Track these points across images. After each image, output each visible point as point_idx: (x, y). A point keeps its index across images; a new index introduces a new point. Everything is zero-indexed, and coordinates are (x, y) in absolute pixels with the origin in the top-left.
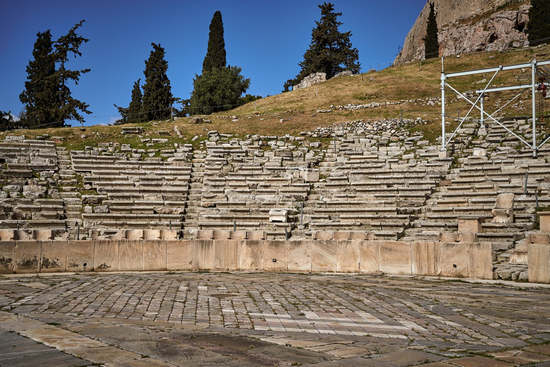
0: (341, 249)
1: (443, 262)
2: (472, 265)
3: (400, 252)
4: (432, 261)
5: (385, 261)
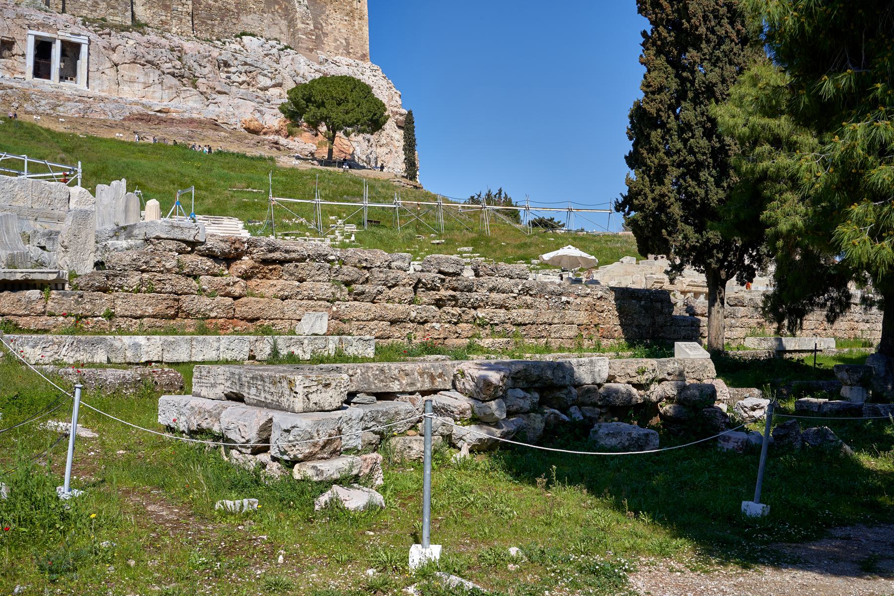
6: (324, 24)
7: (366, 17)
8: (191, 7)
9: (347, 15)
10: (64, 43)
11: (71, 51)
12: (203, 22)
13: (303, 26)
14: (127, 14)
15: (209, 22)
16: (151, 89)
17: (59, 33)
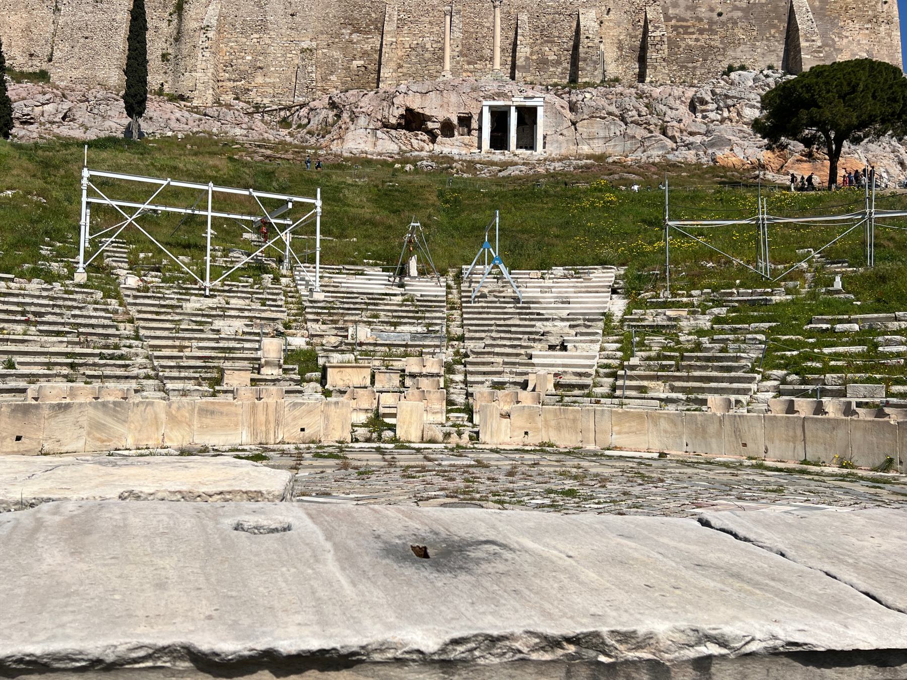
0: (135, 416)
1: (287, 425)
2: (326, 428)
3: (227, 415)
4: (272, 425)
5: (203, 428)
6: (837, 39)
7: (897, 19)
8: (666, 53)
9: (870, 21)
10: (519, 109)
11: (528, 116)
12: (682, 67)
13: (807, 44)
14: (596, 73)
15: (690, 65)
16: (612, 143)
17: (513, 99)
